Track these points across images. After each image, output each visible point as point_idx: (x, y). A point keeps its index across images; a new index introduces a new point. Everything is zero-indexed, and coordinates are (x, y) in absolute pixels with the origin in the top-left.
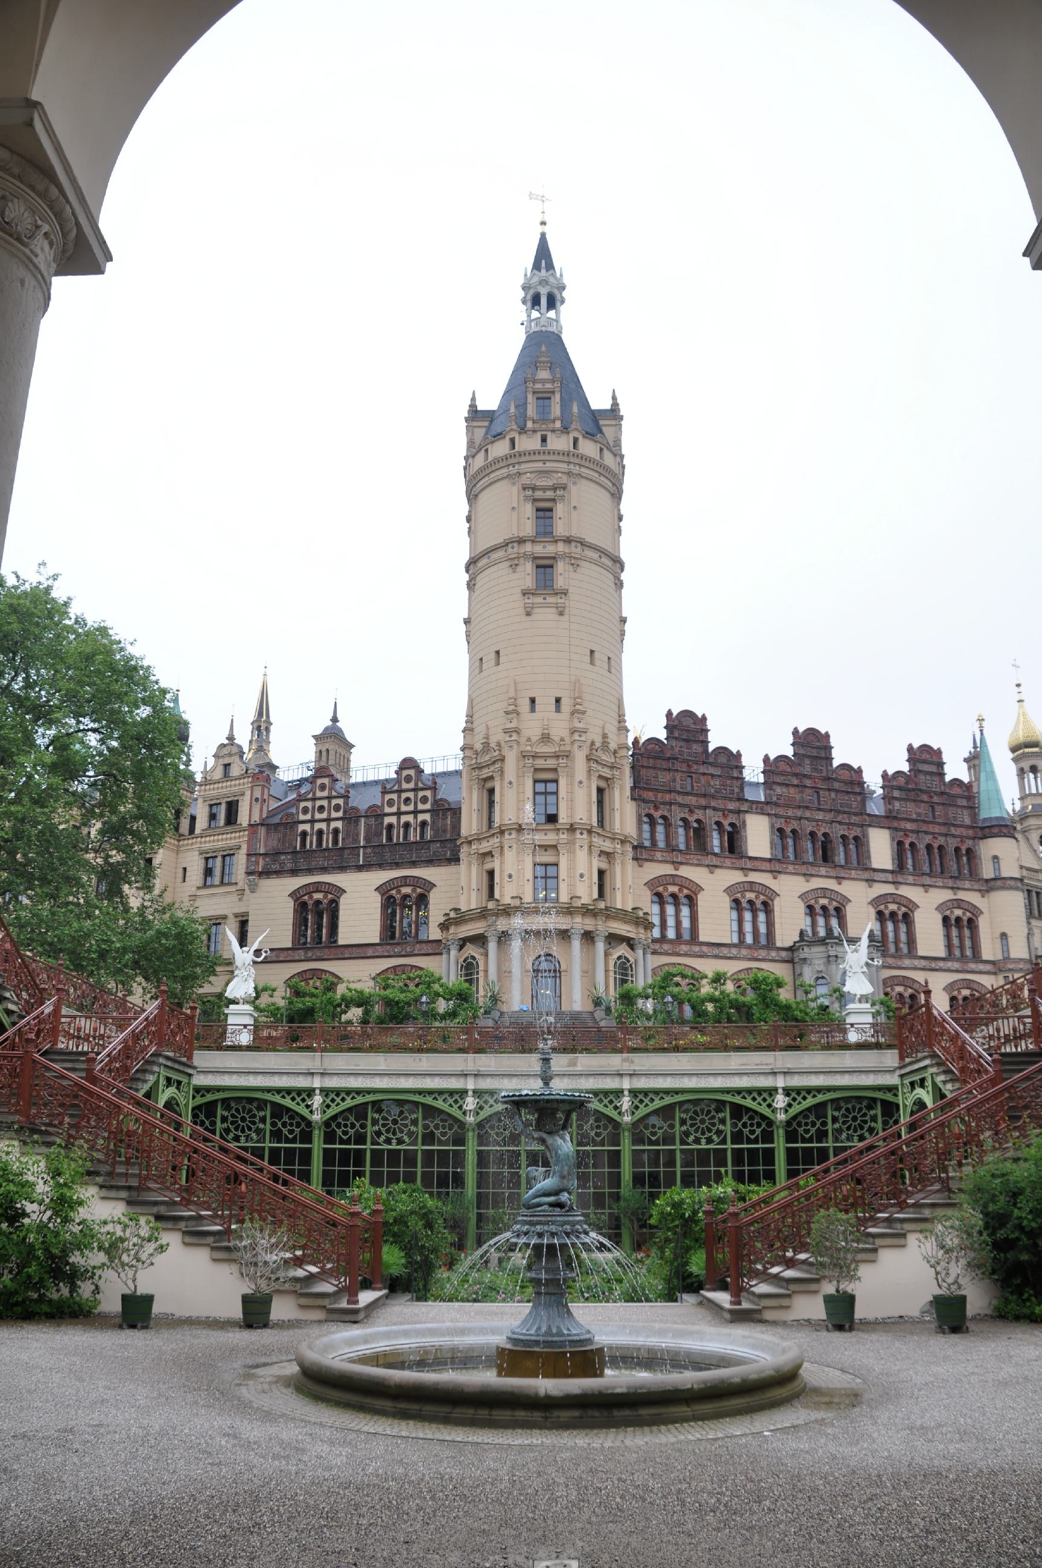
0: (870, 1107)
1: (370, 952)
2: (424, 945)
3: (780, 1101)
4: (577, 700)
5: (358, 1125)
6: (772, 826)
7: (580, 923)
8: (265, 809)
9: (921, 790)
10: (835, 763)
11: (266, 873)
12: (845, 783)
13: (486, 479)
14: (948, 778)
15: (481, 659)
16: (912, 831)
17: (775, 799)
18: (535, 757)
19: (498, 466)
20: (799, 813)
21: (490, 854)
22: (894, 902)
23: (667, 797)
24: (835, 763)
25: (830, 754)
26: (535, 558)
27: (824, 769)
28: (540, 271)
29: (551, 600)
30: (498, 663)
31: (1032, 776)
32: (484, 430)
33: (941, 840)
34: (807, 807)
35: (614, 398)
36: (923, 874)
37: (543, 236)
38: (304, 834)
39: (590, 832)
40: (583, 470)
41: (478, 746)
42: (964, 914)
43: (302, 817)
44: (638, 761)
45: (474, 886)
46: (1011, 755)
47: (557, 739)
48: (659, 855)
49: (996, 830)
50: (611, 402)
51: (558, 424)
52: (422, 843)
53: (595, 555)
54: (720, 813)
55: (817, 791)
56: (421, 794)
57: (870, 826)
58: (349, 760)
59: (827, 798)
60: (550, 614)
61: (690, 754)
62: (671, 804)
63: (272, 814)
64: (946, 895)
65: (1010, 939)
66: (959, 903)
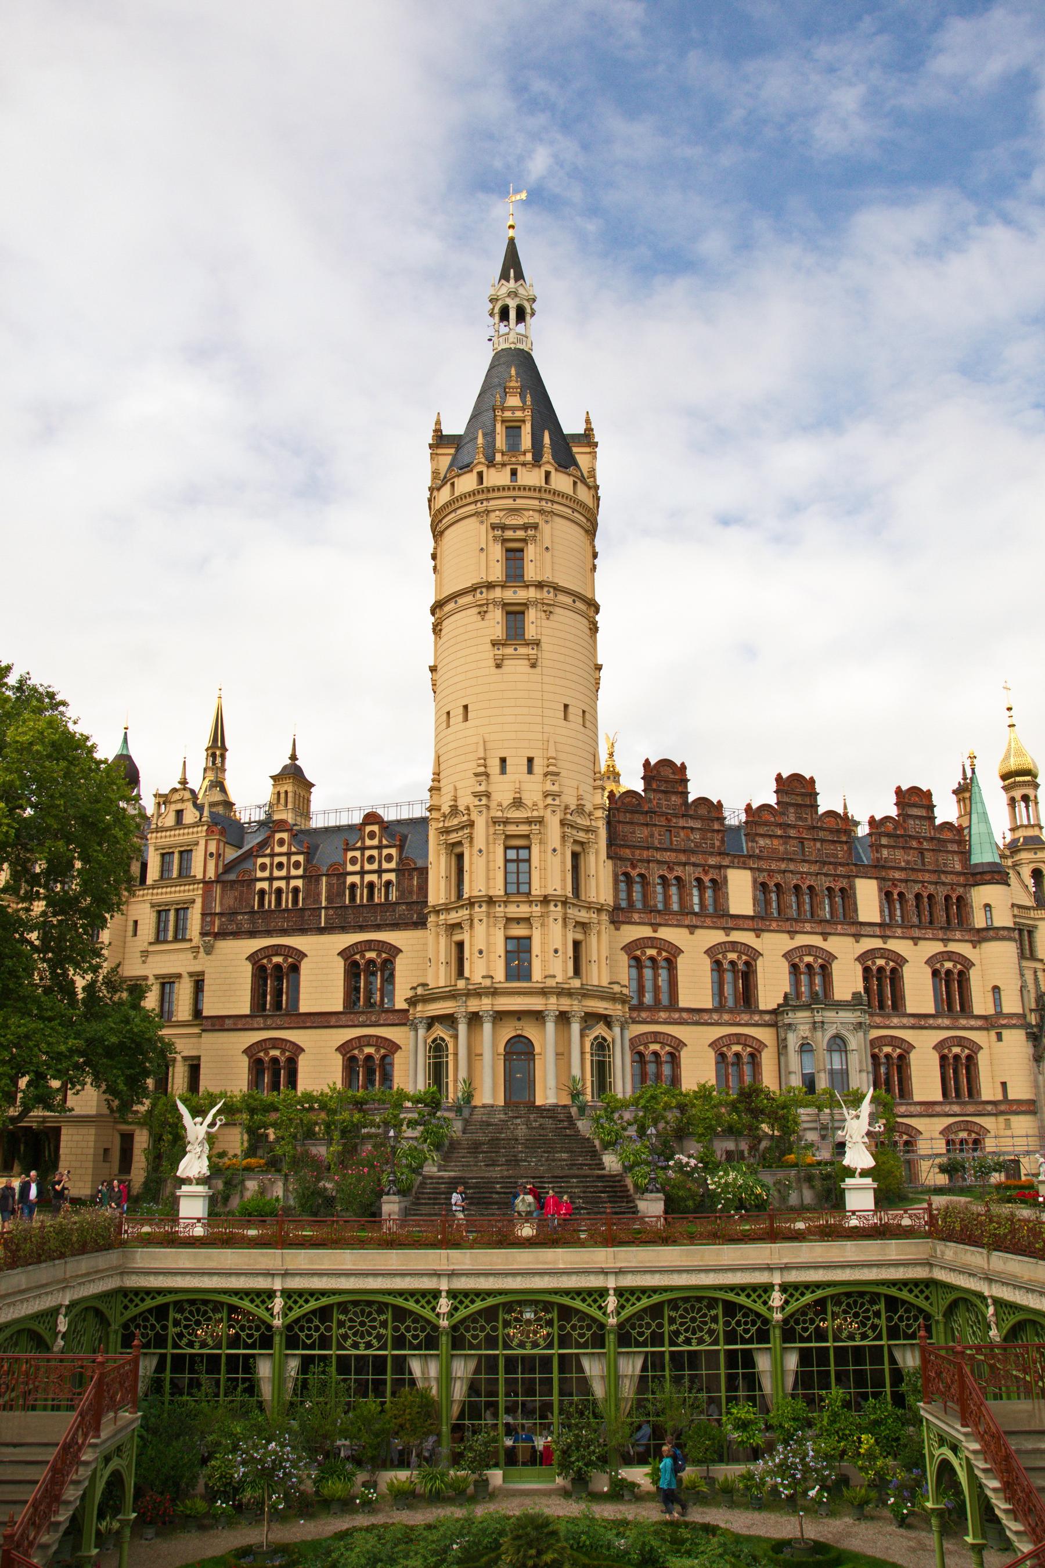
0: (873, 1302)
1: (333, 1021)
2: (390, 1014)
3: (777, 1299)
4: (551, 761)
5: (322, 1328)
6: (755, 881)
7: (553, 1005)
8: (221, 864)
9: (910, 836)
10: (821, 810)
11: (222, 935)
12: (831, 831)
13: (453, 515)
14: (938, 822)
15: (448, 713)
16: (901, 881)
18: (506, 822)
19: (464, 502)
20: (783, 866)
21: (459, 925)
22: (882, 957)
23: (645, 854)
24: (821, 810)
25: (816, 801)
26: (505, 605)
27: (809, 817)
28: (508, 281)
29: (522, 650)
30: (466, 719)
31: (1023, 804)
32: (450, 457)
33: (931, 889)
34: (791, 860)
35: (588, 421)
36: (912, 926)
37: (512, 242)
38: (262, 892)
39: (564, 903)
40: (556, 506)
41: (446, 809)
42: (955, 966)
43: (260, 874)
44: (614, 816)
45: (442, 959)
46: (1001, 784)
47: (529, 803)
48: (636, 917)
49: (988, 877)
50: (584, 426)
51: (529, 457)
52: (388, 905)
53: (568, 600)
54: (700, 869)
55: (801, 841)
56: (385, 852)
57: (857, 876)
58: (309, 801)
59: (813, 849)
60: (523, 666)
61: (668, 807)
62: (649, 861)
63: (229, 868)
64: (936, 947)
65: (1002, 993)
66: (950, 956)
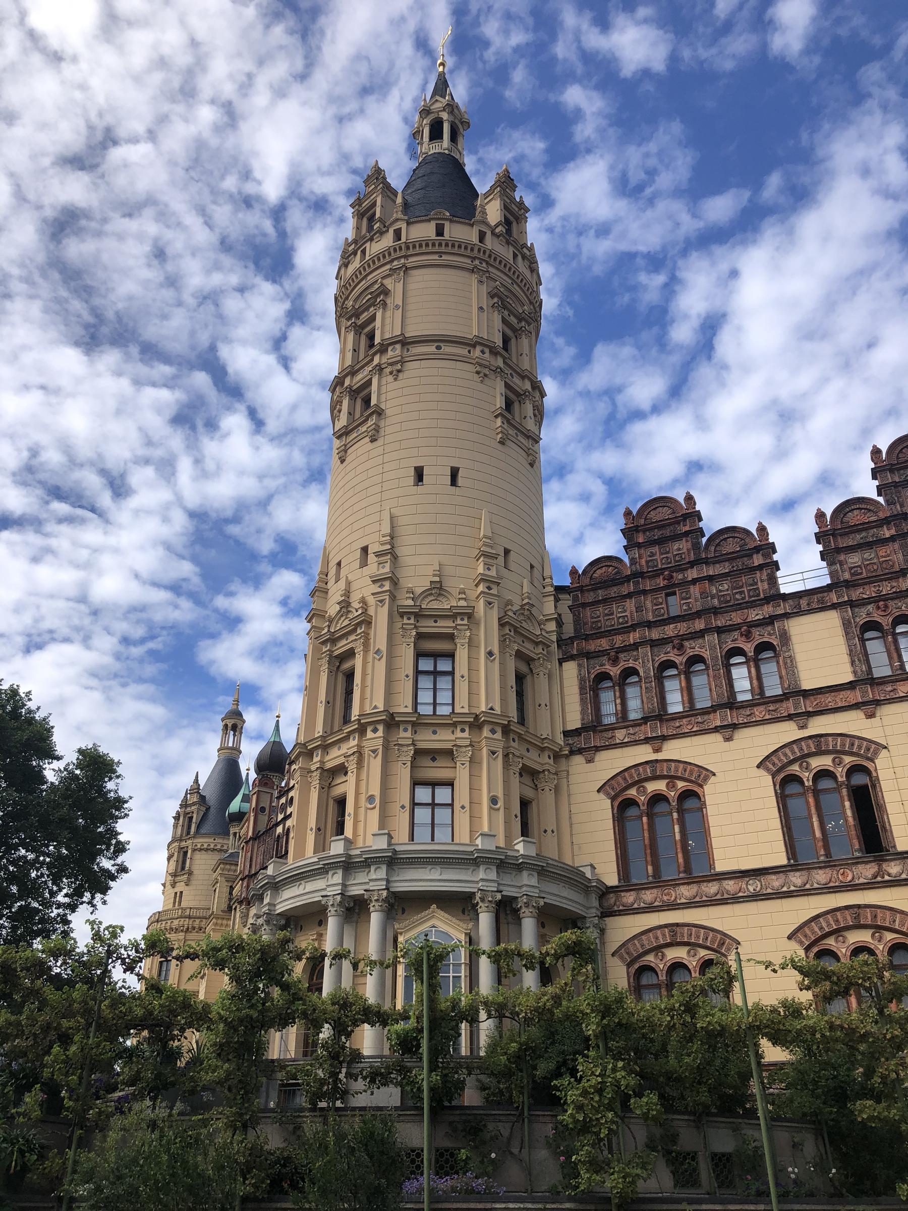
17: (847, 576)
